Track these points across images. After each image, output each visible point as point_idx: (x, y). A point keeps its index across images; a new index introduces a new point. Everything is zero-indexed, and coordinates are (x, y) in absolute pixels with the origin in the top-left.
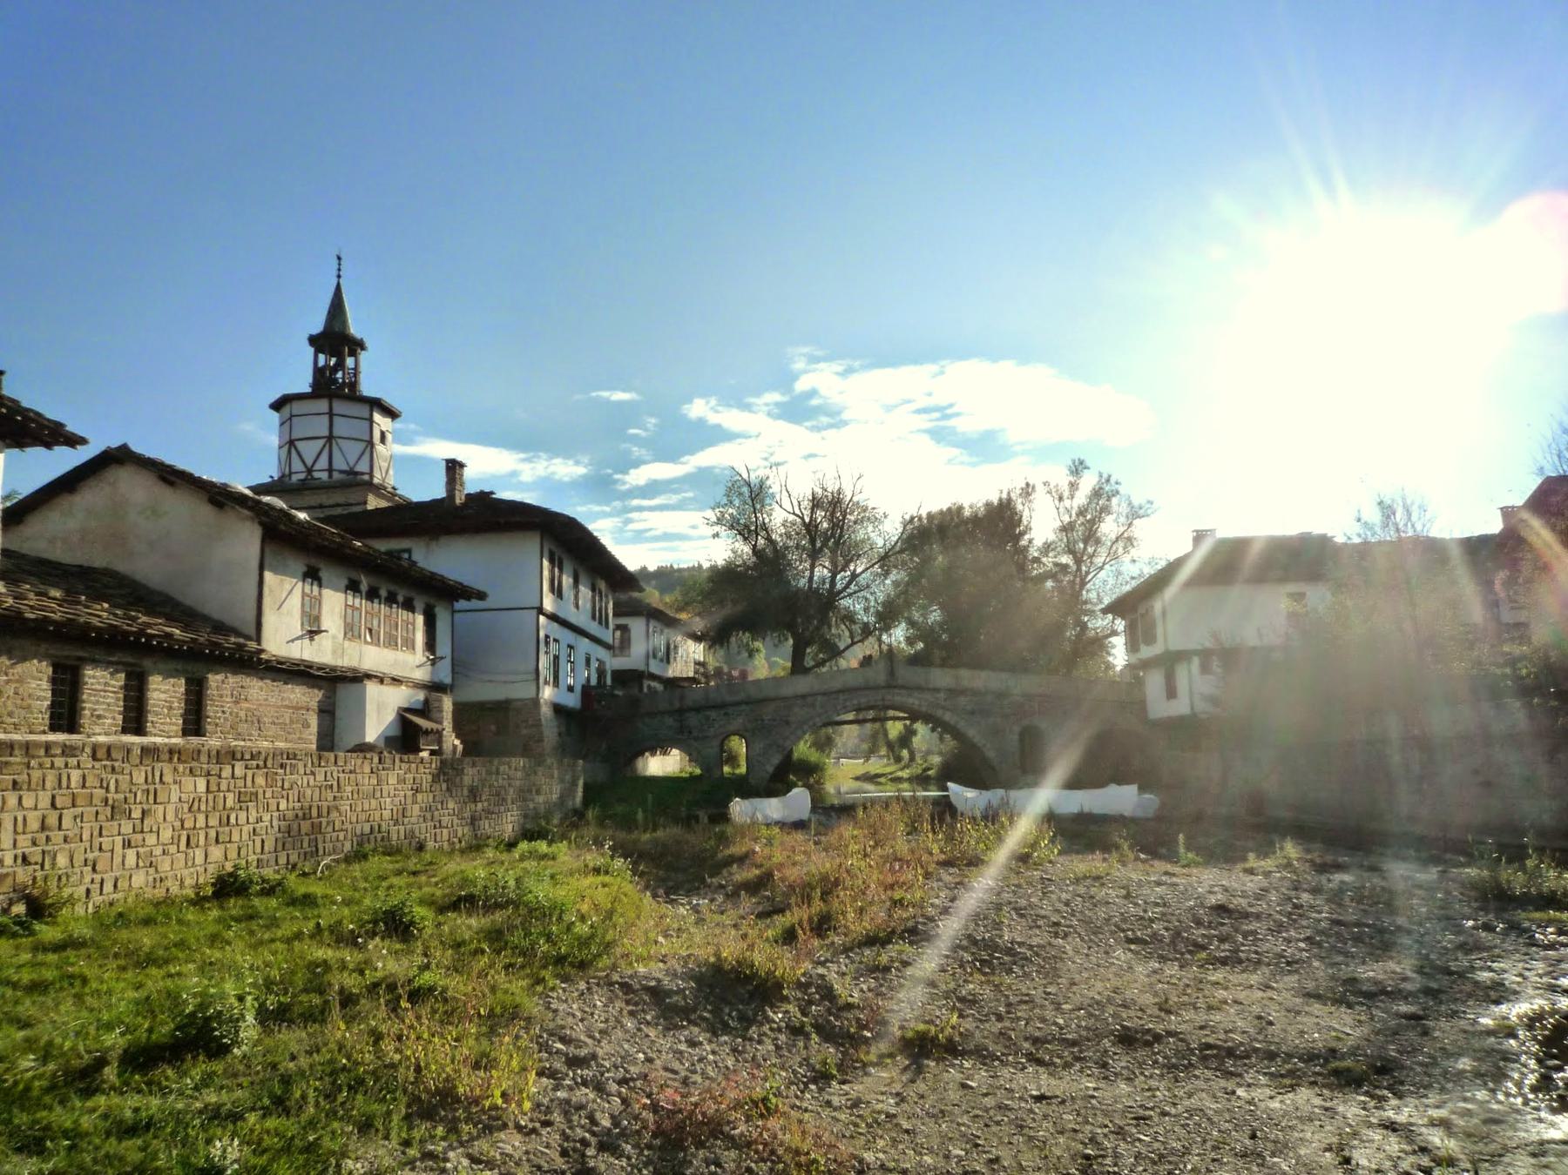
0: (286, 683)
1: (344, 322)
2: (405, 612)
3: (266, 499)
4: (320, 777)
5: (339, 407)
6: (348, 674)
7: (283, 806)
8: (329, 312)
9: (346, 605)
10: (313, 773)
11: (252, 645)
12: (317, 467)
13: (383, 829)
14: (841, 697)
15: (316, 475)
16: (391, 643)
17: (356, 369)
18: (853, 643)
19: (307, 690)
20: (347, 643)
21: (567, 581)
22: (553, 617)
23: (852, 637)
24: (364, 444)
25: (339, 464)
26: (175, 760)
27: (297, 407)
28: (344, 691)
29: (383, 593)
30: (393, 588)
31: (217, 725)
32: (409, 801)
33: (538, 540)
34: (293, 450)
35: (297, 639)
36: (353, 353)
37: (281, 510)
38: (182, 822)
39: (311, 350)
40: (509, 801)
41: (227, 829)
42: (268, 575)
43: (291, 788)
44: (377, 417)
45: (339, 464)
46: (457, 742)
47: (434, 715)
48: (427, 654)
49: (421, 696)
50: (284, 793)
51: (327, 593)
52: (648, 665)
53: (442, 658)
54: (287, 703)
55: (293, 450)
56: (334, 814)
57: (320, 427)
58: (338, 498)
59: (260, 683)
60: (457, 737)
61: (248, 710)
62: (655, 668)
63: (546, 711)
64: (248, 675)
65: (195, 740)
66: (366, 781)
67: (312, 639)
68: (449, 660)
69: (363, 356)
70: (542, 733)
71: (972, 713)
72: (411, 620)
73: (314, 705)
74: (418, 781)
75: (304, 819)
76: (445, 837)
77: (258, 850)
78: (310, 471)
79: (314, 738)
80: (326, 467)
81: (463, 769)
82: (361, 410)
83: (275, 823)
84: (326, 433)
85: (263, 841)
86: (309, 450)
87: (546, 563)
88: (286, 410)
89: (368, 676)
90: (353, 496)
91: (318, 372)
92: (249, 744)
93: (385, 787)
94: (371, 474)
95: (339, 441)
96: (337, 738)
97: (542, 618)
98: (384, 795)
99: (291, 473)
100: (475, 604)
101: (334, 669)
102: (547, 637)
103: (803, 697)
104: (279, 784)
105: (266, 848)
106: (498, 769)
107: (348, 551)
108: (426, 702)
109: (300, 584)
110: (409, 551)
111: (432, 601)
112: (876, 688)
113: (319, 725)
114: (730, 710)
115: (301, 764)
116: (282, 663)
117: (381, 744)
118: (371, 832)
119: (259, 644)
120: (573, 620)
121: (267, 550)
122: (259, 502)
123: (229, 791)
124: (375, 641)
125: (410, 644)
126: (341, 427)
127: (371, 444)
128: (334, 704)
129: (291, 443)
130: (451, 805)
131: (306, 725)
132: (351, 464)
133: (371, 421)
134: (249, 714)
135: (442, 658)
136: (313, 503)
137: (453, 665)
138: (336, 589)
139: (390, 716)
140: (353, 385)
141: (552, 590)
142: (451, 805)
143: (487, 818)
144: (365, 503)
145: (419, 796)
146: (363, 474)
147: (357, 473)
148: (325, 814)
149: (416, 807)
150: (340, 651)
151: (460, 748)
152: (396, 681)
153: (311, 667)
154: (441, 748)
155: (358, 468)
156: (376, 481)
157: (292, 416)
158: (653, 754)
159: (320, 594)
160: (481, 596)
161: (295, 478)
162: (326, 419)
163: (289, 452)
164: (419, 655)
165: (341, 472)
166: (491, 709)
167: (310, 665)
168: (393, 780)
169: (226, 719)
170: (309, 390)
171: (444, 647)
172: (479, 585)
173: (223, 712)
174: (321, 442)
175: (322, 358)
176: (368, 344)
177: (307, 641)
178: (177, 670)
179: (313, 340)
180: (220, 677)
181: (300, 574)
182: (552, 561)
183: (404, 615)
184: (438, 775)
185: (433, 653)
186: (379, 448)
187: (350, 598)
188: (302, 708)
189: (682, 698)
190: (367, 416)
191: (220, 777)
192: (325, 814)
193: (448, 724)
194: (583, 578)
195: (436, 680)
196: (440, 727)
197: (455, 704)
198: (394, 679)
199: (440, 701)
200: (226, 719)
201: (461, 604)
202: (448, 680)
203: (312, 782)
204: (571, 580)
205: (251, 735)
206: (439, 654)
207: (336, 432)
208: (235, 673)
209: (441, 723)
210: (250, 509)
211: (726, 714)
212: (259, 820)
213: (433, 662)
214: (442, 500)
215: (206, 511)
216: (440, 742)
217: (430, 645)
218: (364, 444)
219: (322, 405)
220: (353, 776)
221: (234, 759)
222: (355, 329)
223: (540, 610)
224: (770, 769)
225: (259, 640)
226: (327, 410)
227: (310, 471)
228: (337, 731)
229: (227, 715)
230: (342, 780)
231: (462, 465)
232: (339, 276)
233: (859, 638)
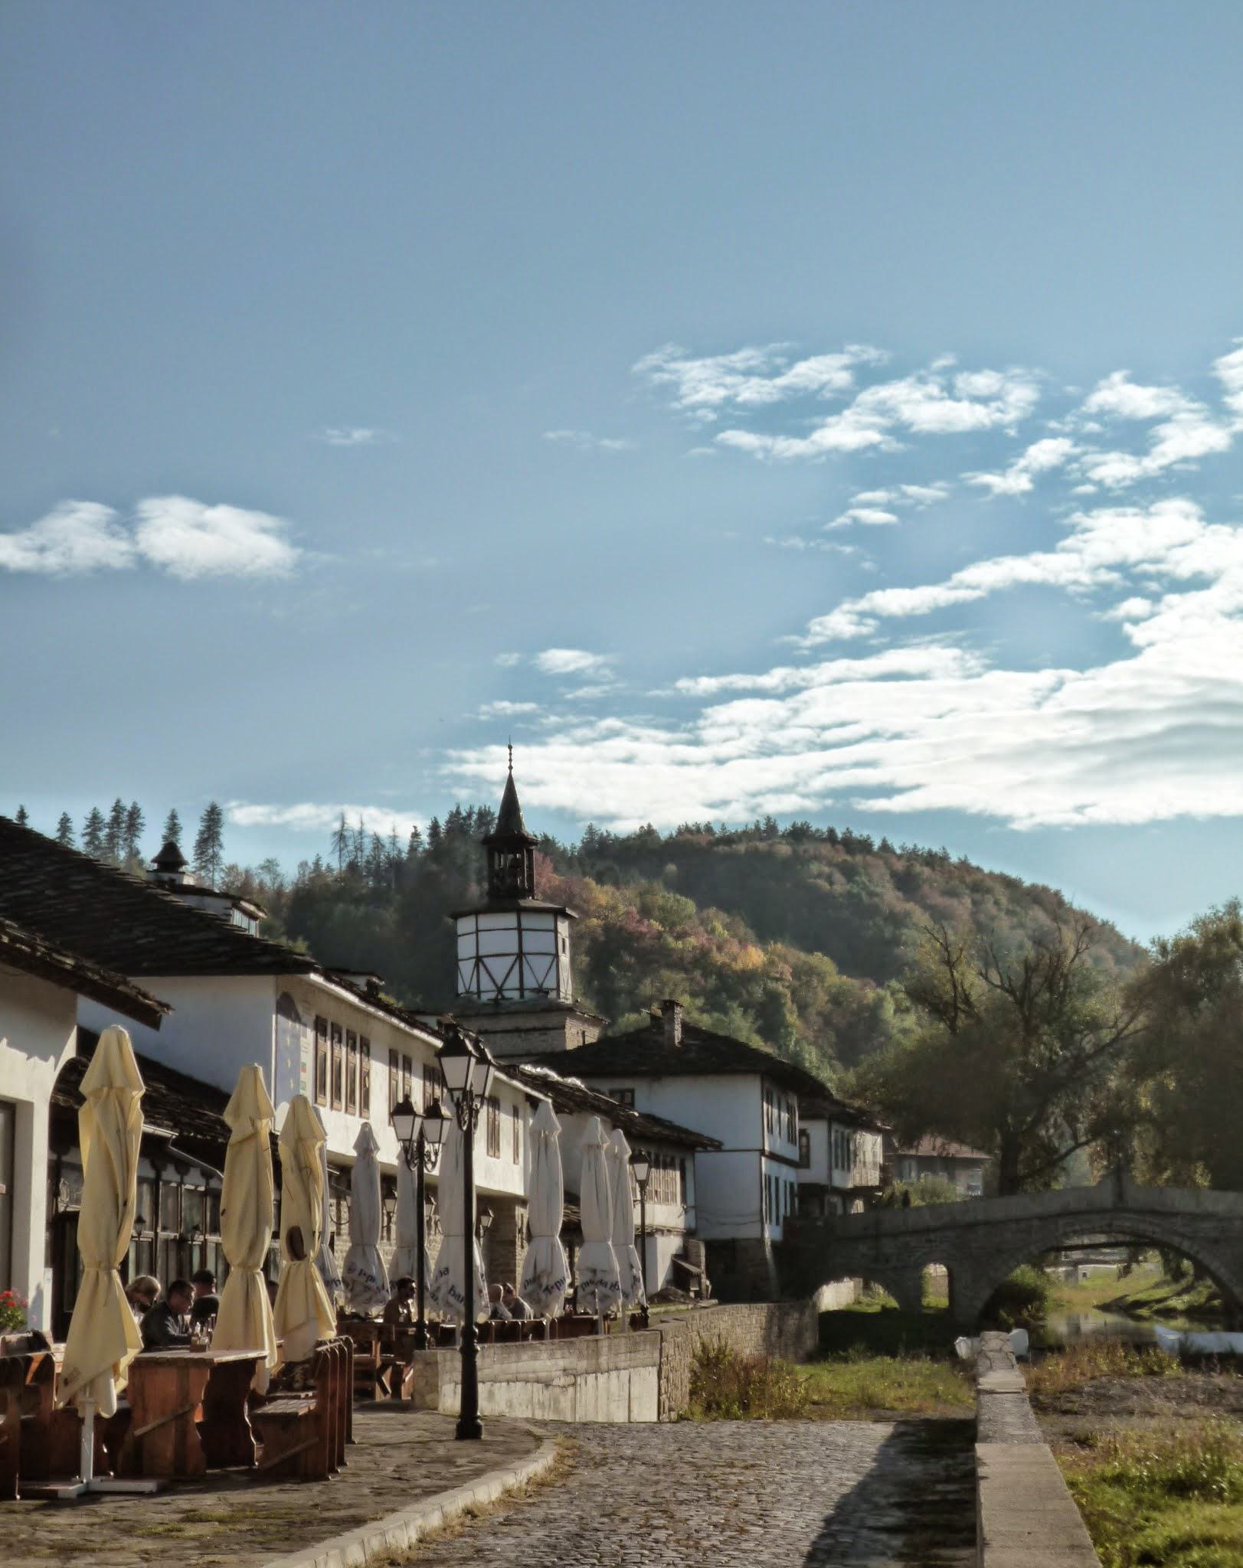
1: (518, 822)
12: (507, 985)
14: (1061, 1222)
15: (507, 994)
18: (1078, 1145)
22: (773, 1157)
23: (1075, 1137)
25: (530, 982)
45: (530, 982)
46: (708, 1283)
47: (693, 1259)
52: (830, 1177)
55: (482, 968)
57: (509, 942)
71: (1216, 1241)
78: (500, 990)
80: (517, 985)
84: (516, 950)
86: (499, 967)
89: (657, 1230)
94: (558, 989)
95: (529, 957)
97: (763, 1159)
99: (479, 992)
103: (1018, 1221)
110: (632, 1091)
112: (1102, 1211)
114: (932, 1236)
126: (531, 942)
133: (556, 931)
144: (563, 1027)
146: (552, 989)
155: (545, 986)
157: (477, 931)
161: (485, 997)
162: (516, 932)
163: (477, 965)
164: (677, 1207)
165: (533, 990)
171: (691, 1201)
174: (513, 958)
182: (768, 1103)
183: (670, 1172)
190: (552, 927)
198: (669, 1231)
199: (699, 1247)
202: (693, 1225)
207: (525, 949)
211: (929, 1241)
216: (700, 1284)
217: (684, 1200)
218: (549, 959)
219: (510, 920)
223: (762, 1152)
224: (979, 1305)
226: (515, 924)
227: (500, 990)
233: (1083, 1139)
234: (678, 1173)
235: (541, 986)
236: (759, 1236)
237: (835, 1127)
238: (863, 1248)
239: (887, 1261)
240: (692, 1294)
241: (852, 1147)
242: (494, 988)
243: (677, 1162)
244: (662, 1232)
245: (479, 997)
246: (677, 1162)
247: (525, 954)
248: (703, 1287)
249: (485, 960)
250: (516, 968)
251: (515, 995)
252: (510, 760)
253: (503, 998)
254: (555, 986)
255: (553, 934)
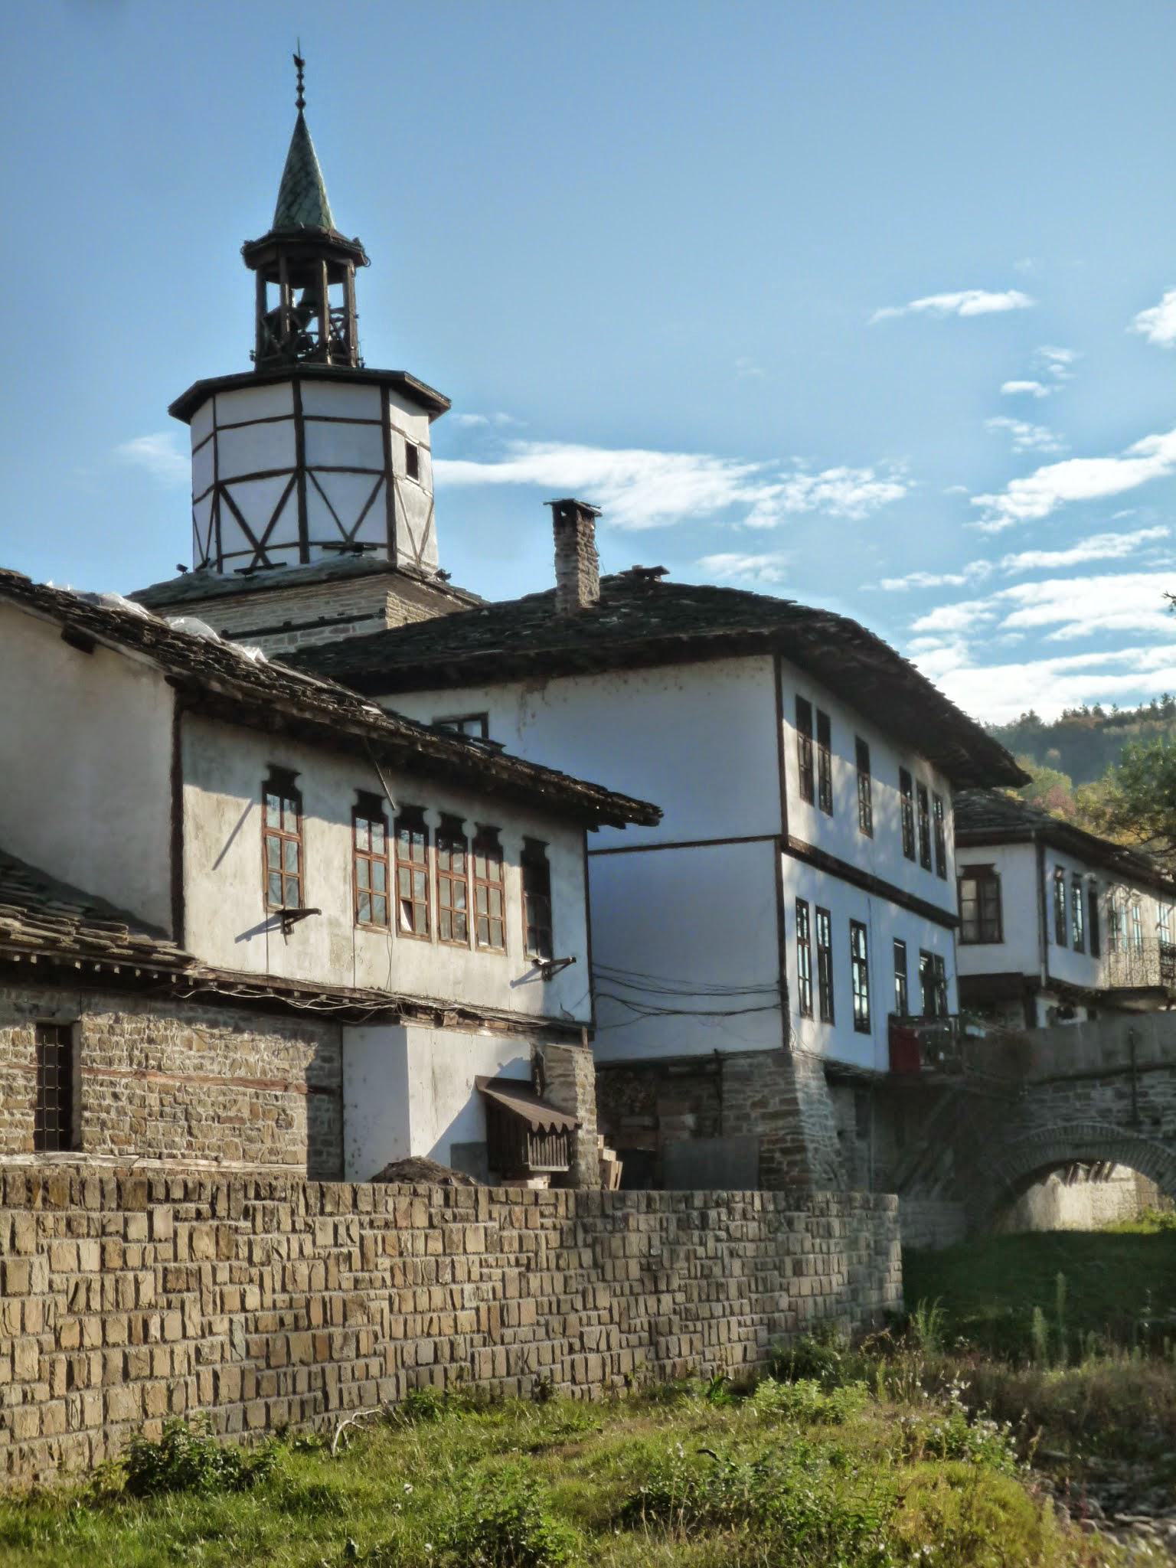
0: (238, 1030)
1: (318, 206)
2: (481, 862)
3: (177, 623)
4: (325, 1238)
5: (318, 398)
6: (368, 1006)
7: (252, 1301)
8: (284, 187)
9: (355, 850)
10: (310, 1229)
11: (167, 947)
12: (273, 540)
13: (461, 1352)
15: (274, 557)
16: (457, 932)
17: (347, 310)
19: (282, 1044)
20: (360, 936)
21: (841, 770)
22: (812, 857)
24: (375, 479)
25: (323, 528)
26: (39, 1203)
27: (229, 407)
28: (359, 1042)
29: (432, 820)
30: (453, 807)
31: (103, 1124)
32: (513, 1290)
33: (767, 678)
34: (224, 506)
35: (258, 930)
36: (339, 275)
37: (208, 646)
38: (57, 1333)
39: (251, 276)
40: (733, 1291)
41: (144, 1349)
42: (191, 793)
43: (268, 1262)
44: (399, 416)
45: (323, 528)
46: (610, 1155)
47: (556, 1094)
48: (534, 954)
49: (523, 1049)
50: (254, 1271)
51: (313, 825)
52: (1045, 960)
53: (566, 963)
54: (241, 1073)
55: (224, 506)
56: (358, 1319)
58: (323, 606)
59: (187, 1032)
60: (610, 1143)
61: (165, 1090)
62: (1064, 967)
63: (807, 1079)
64: (162, 1014)
65: (61, 1158)
66: (420, 1245)
67: (287, 930)
68: (580, 968)
69: (361, 278)
70: (797, 1131)
72: (494, 877)
73: (298, 1076)
74: (529, 1244)
75: (297, 1328)
76: (595, 1373)
77: (208, 1395)
78: (260, 548)
79: (302, 1151)
80: (294, 536)
81: (625, 1219)
82: (364, 401)
83: (239, 1337)
84: (291, 461)
85: (216, 1376)
87: (790, 732)
88: (204, 415)
89: (409, 1009)
90: (355, 599)
91: (268, 322)
92: (169, 1164)
93: (460, 1259)
94: (391, 546)
95: (316, 474)
96: (349, 1148)
97: (786, 860)
98: (461, 1274)
99: (221, 557)
100: (635, 833)
101: (336, 995)
102: (801, 903)
104: (244, 1252)
105: (223, 1391)
106: (704, 1218)
107: (356, 731)
108: (537, 1062)
109: (257, 809)
110: (482, 718)
111: (539, 833)
113: (312, 1121)
115: (284, 1209)
116: (229, 986)
117: (445, 1161)
118: (436, 1361)
119: (181, 945)
120: (859, 862)
121: (187, 739)
122: (164, 631)
123: (144, 1266)
124: (420, 929)
125: (493, 934)
126: (325, 444)
127: (386, 475)
128: (341, 1073)
129: (219, 489)
130: (604, 1299)
131: (284, 1122)
132: (349, 527)
133: (385, 425)
134: (168, 1099)
135: (566, 963)
136: (272, 622)
137: (592, 977)
138: (332, 817)
139: (459, 1099)
140: (343, 348)
141: (808, 793)
142: (604, 1299)
143: (684, 1329)
144: (382, 613)
145: (534, 1281)
146: (373, 547)
147: (359, 548)
148: (338, 1318)
149: (529, 1304)
150: (347, 957)
151: (617, 1168)
152: (469, 1017)
153: (289, 993)
154: (574, 1167)
155: (359, 538)
156: (402, 561)
157: (217, 429)
158: (1069, 1178)
159: (300, 829)
160: (648, 815)
161: (230, 567)
162: (289, 426)
165: (327, 546)
166: (681, 1077)
167: (285, 988)
168: (475, 1243)
169: (121, 1112)
170: (250, 367)
172: (639, 791)
173: (115, 1096)
174: (286, 479)
175: (273, 290)
176: (369, 251)
177: (277, 935)
178: (19, 1009)
179: (253, 254)
180: (104, 1020)
181: (257, 789)
182: (803, 725)
183: (477, 865)
184: (573, 1231)
185: (547, 951)
186: (405, 485)
187: (362, 835)
188: (273, 1084)
189: (1133, 1041)
190: (378, 417)
191: (125, 1238)
192: (338, 1318)
193: (586, 1115)
194: (881, 758)
195: (557, 1013)
196: (570, 1122)
197: (599, 1067)
198: (463, 1014)
199: (570, 1060)
200: (121, 1112)
201: (605, 836)
203: (308, 1250)
204: (851, 767)
205: (172, 1145)
206: (559, 954)
207: (311, 460)
208: (134, 1012)
209: (571, 1112)
210: (148, 649)
212: (207, 1330)
213: (548, 973)
214: (549, 596)
215: (61, 657)
216: (571, 1156)
218: (375, 479)
219: (279, 399)
220: (392, 1234)
221: (150, 1198)
222: (341, 222)
223: (783, 843)
225: (179, 934)
226: (289, 409)
227: (260, 548)
228: (348, 1131)
229: (124, 1102)
230: (369, 1244)
231: (589, 514)
232: (301, 104)
234: (514, 876)
235: (349, 538)
236: (778, 1044)
237: (1052, 859)
238: (1104, 1096)
239: (1157, 1122)
240: (539, 1184)
241: (1103, 915)
242: (249, 546)
243: (511, 841)
244: (438, 1020)
245: (220, 570)
246: (511, 841)
247: (310, 470)
248: (586, 1164)
249: (232, 489)
250: (293, 499)
251: (292, 557)
252: (301, 89)
253: (269, 566)
254: (383, 539)
255: (378, 429)
